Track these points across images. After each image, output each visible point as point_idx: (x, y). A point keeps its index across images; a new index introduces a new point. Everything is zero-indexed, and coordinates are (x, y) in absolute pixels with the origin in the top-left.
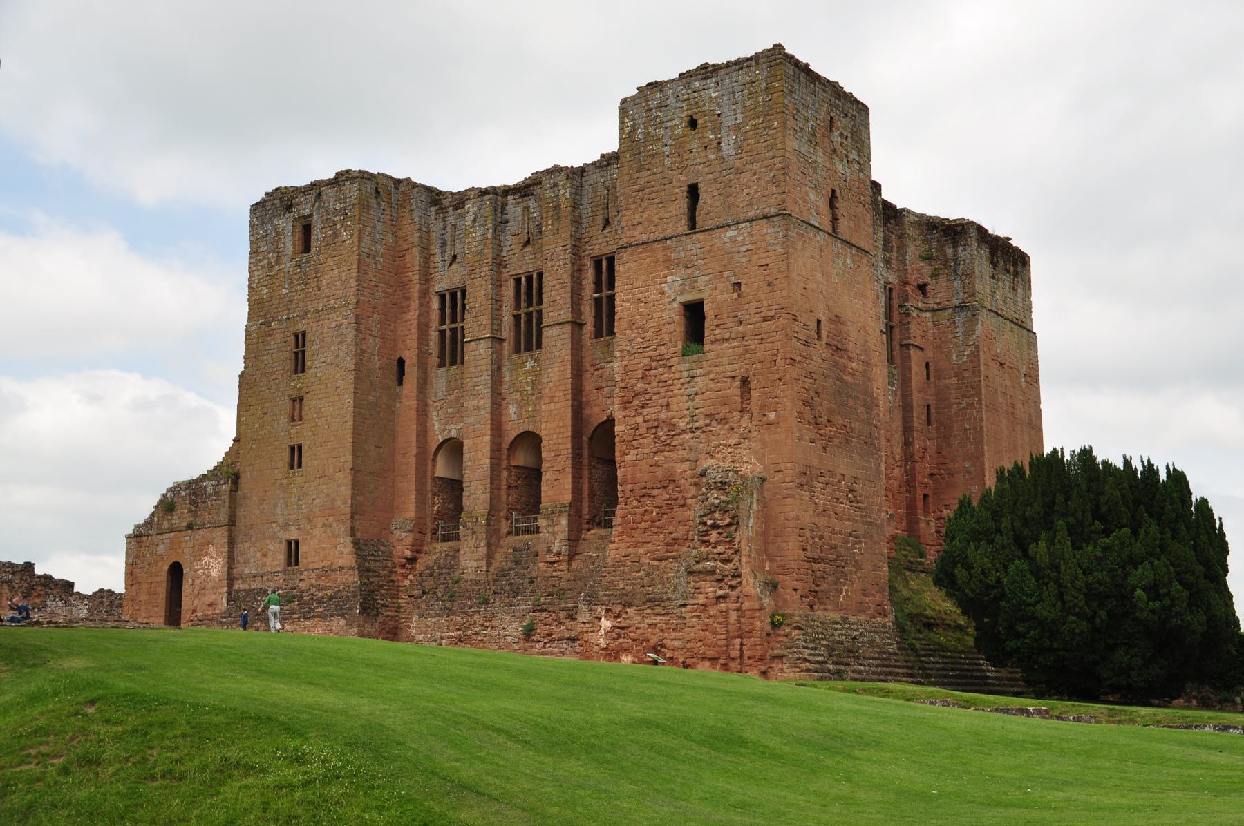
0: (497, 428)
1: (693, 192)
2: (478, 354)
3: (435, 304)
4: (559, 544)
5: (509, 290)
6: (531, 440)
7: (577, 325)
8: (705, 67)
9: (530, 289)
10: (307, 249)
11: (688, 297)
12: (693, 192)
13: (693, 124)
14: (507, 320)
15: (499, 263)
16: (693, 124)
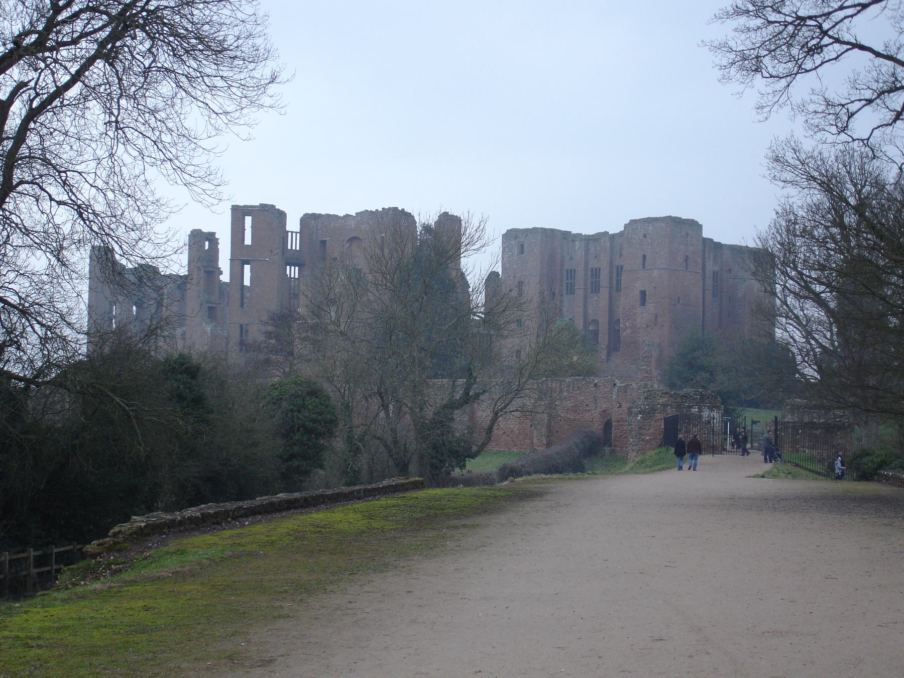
0: (585, 316)
1: (644, 256)
2: (580, 293)
3: (565, 273)
4: (604, 357)
5: (589, 273)
6: (596, 322)
7: (611, 288)
8: (648, 218)
9: (596, 273)
10: (522, 252)
11: (643, 289)
12: (644, 256)
13: (645, 236)
14: (589, 283)
15: (587, 263)
16: (645, 236)
